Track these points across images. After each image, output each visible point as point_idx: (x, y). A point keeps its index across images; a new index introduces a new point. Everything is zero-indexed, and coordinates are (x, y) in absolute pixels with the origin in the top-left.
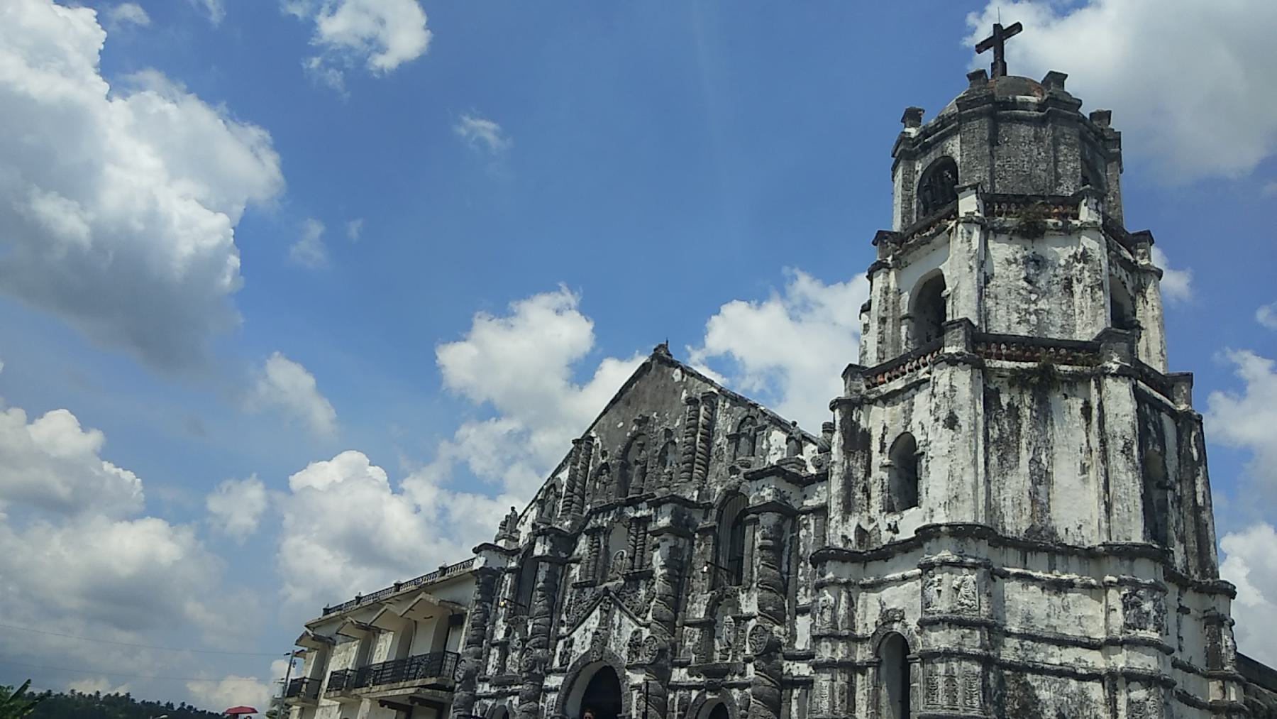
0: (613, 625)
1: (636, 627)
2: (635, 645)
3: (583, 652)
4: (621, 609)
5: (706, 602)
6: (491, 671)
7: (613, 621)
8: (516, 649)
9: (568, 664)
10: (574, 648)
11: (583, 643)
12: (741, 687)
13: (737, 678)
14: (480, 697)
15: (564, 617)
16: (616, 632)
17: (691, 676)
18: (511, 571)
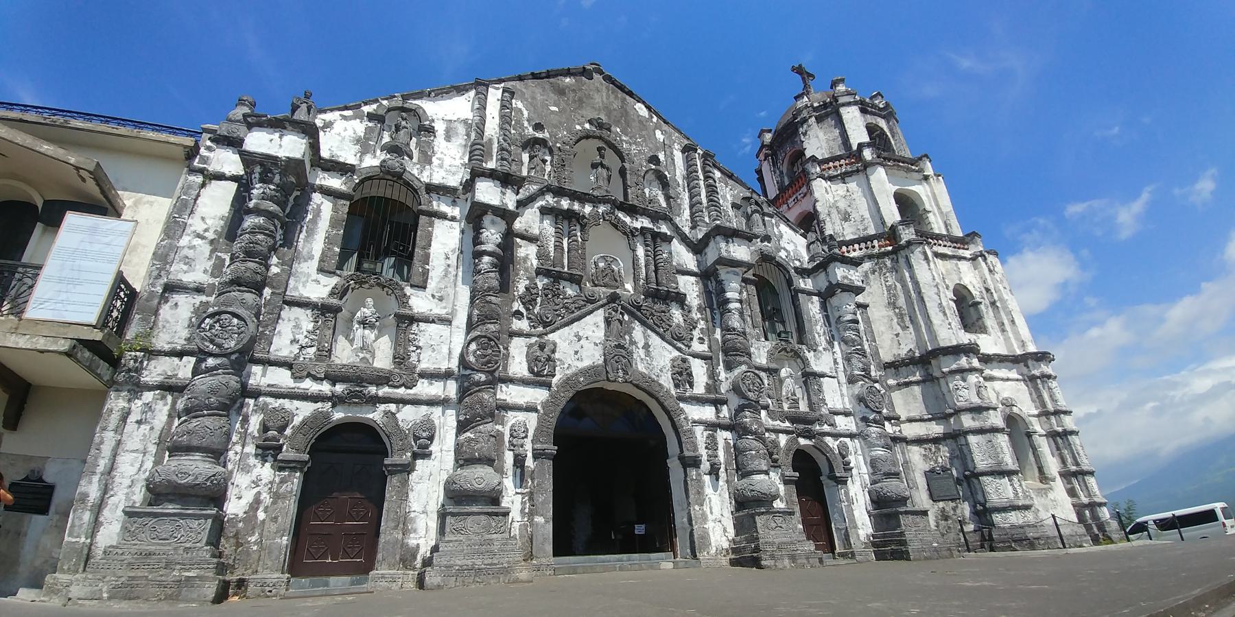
0: (633, 343)
1: (676, 353)
2: (683, 375)
3: (581, 365)
4: (643, 323)
5: (766, 350)
6: (282, 345)
7: (631, 337)
8: (372, 327)
9: (553, 376)
10: (557, 355)
11: (576, 353)
12: (836, 436)
13: (826, 428)
14: (256, 394)
15: (517, 306)
16: (642, 352)
17: (773, 419)
18: (327, 192)
